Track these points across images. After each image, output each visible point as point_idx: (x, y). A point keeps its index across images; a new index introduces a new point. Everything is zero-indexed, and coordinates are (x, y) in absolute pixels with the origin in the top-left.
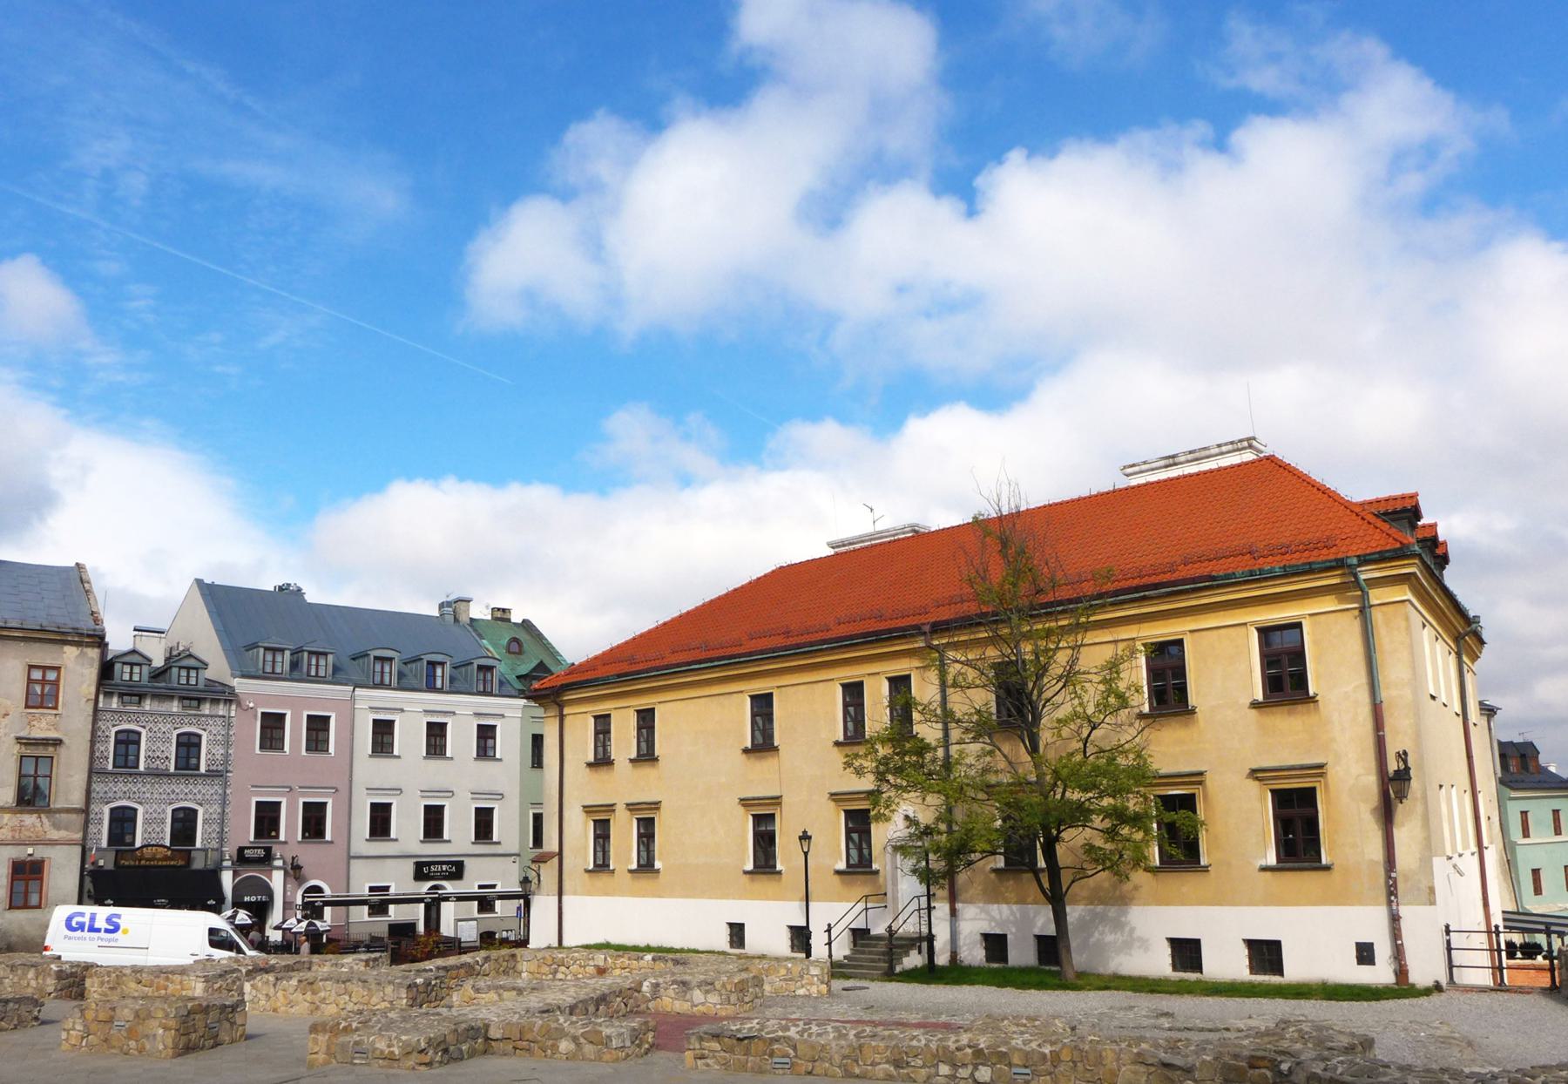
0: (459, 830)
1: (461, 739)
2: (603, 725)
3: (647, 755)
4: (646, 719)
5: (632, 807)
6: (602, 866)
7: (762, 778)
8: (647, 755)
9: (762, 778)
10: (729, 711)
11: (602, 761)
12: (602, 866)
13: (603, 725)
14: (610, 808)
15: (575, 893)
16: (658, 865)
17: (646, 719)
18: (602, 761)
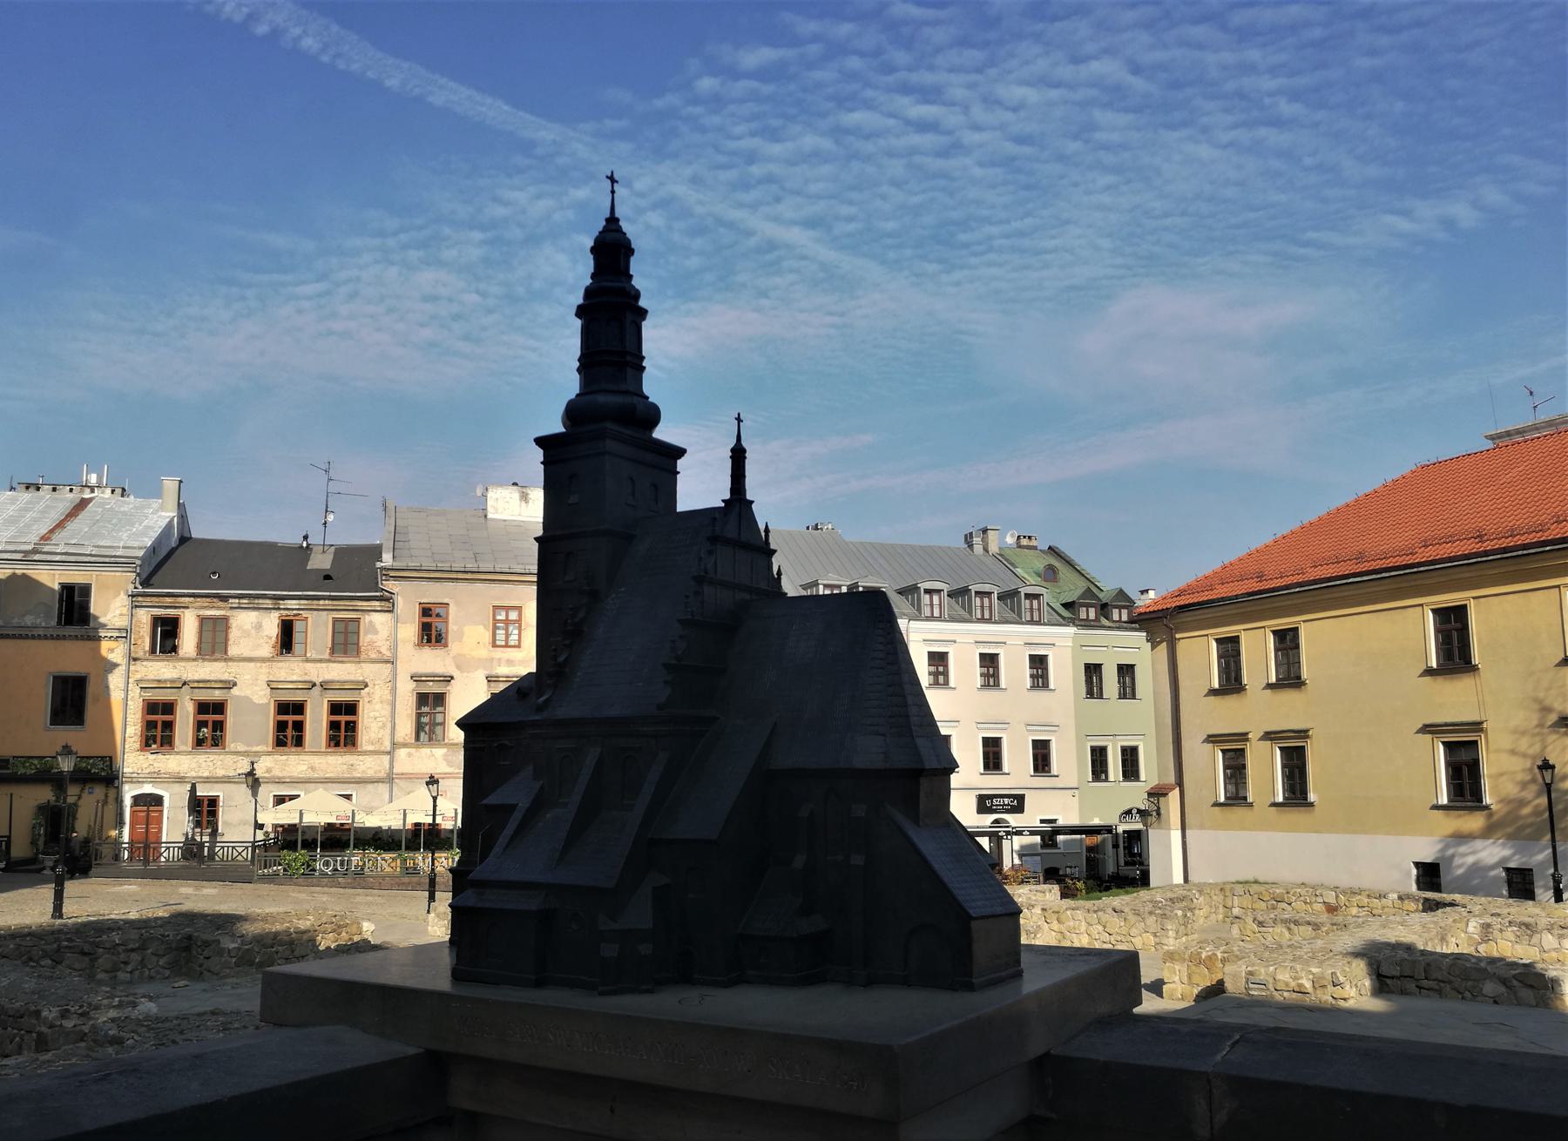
0: (1017, 759)
1: (1014, 670)
2: (1230, 650)
3: (1290, 679)
4: (1287, 641)
5: (1269, 736)
6: (1237, 798)
7: (1454, 700)
8: (1290, 679)
9: (1454, 700)
10: (1413, 627)
11: (1232, 682)
12: (1237, 798)
13: (1230, 650)
14: (1243, 737)
15: (1202, 827)
16: (1312, 797)
17: (1287, 641)
18: (1232, 682)
